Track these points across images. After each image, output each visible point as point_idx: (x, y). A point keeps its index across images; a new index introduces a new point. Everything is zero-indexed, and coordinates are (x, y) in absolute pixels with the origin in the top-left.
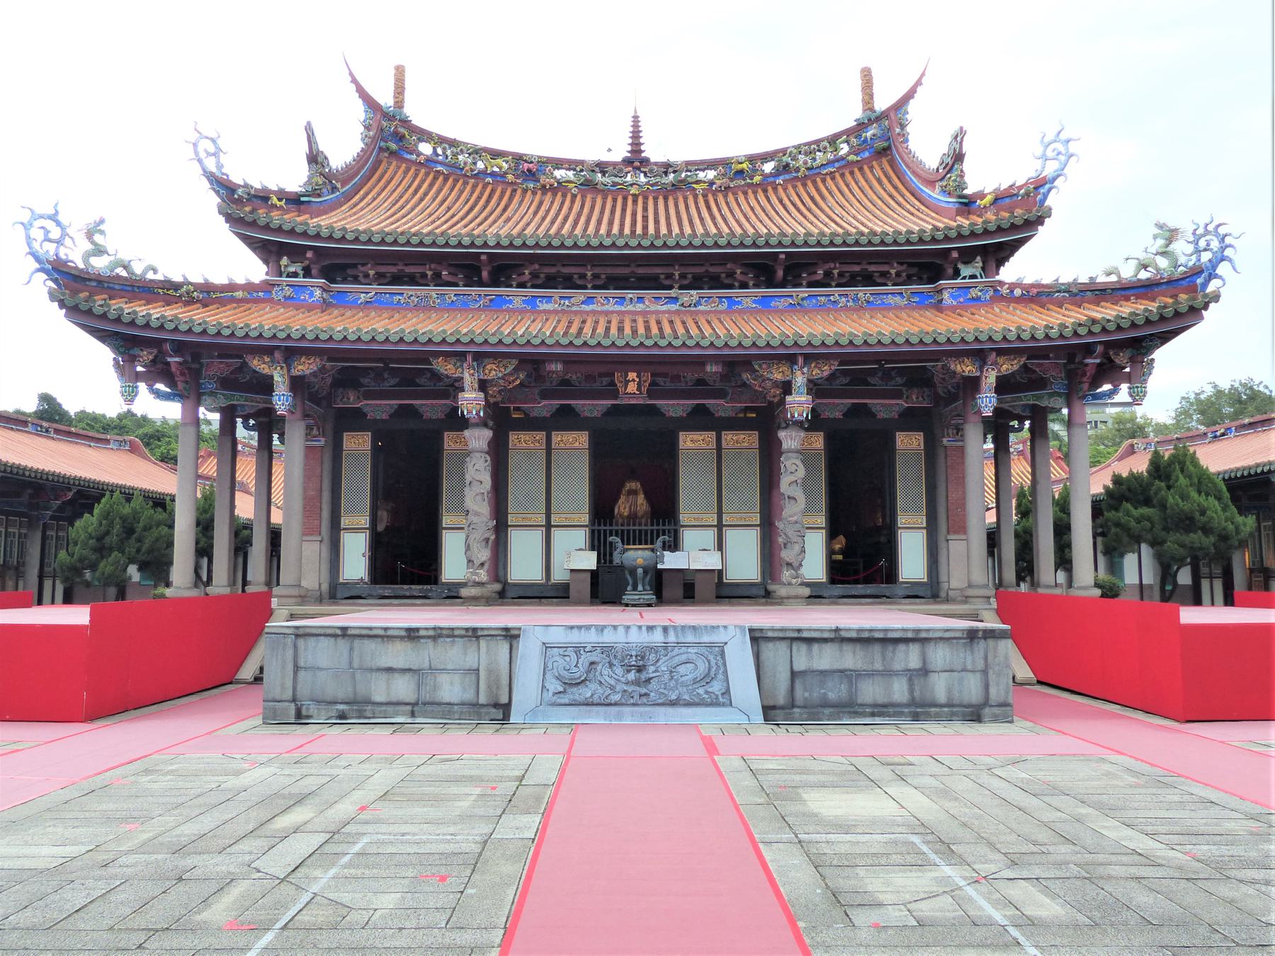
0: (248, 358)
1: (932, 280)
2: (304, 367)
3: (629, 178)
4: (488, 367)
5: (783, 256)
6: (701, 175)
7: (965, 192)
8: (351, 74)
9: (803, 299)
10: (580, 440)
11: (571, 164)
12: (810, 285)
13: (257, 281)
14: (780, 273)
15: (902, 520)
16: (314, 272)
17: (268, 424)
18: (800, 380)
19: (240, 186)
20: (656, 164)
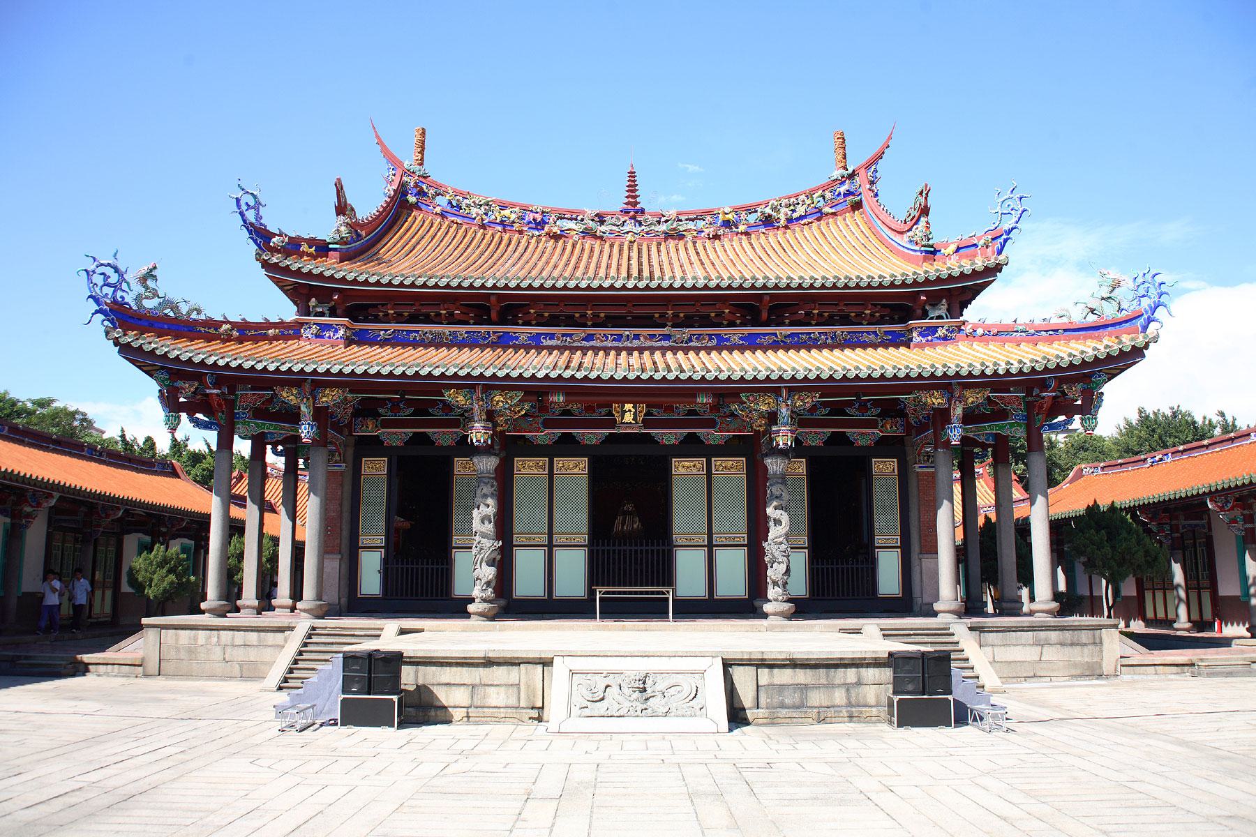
0: (277, 389)
1: (904, 320)
2: (328, 398)
3: (627, 228)
6: (691, 225)
7: (931, 242)
8: (377, 136)
9: (788, 336)
12: (792, 324)
14: (764, 315)
15: (879, 540)
16: (339, 311)
17: (293, 449)
18: (784, 411)
19: (275, 235)
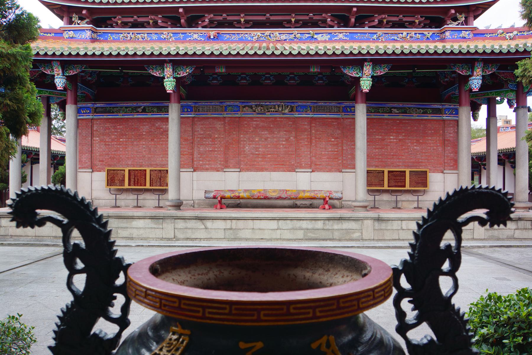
5: (355, 9)
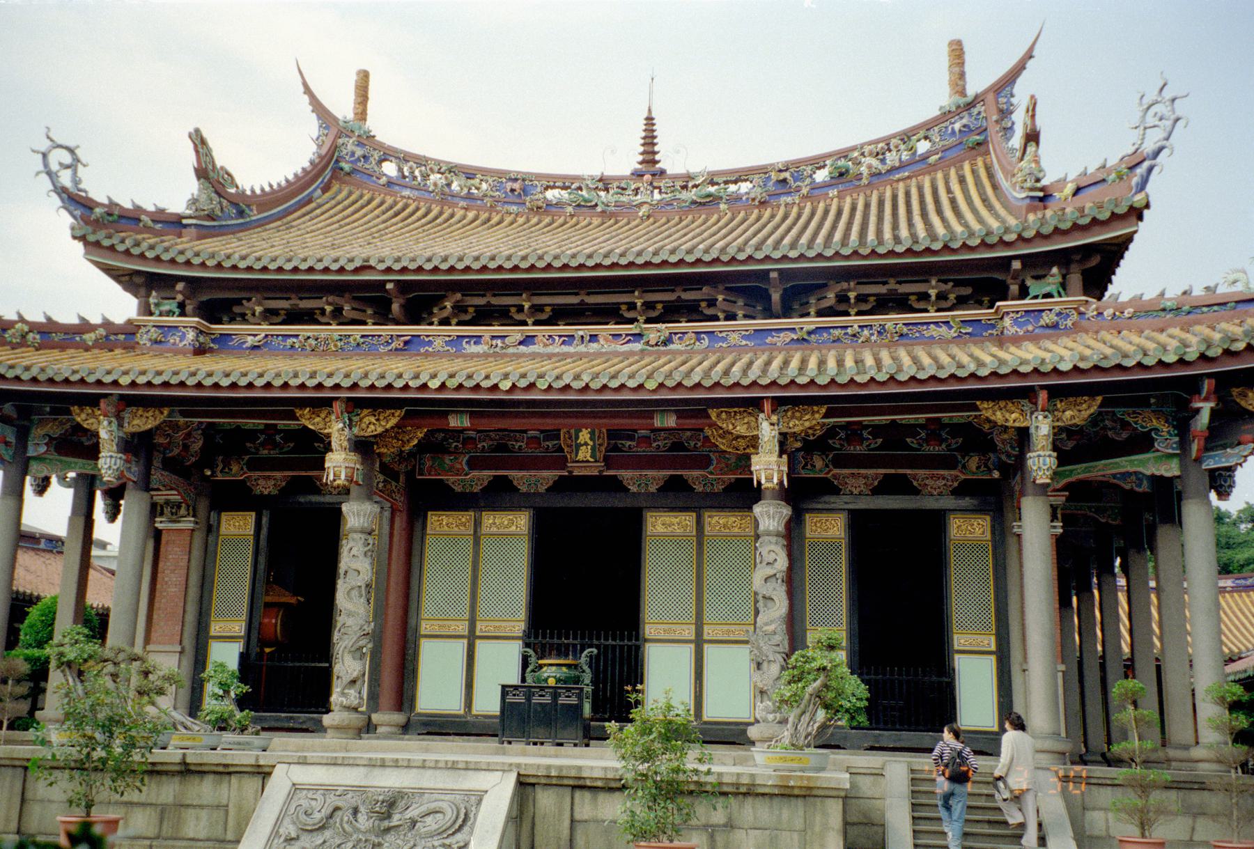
4: (366, 420)
9: (809, 333)
10: (520, 522)
11: (565, 183)
12: (820, 314)
13: (119, 319)
14: (776, 297)
16: (189, 308)
20: (675, 177)
